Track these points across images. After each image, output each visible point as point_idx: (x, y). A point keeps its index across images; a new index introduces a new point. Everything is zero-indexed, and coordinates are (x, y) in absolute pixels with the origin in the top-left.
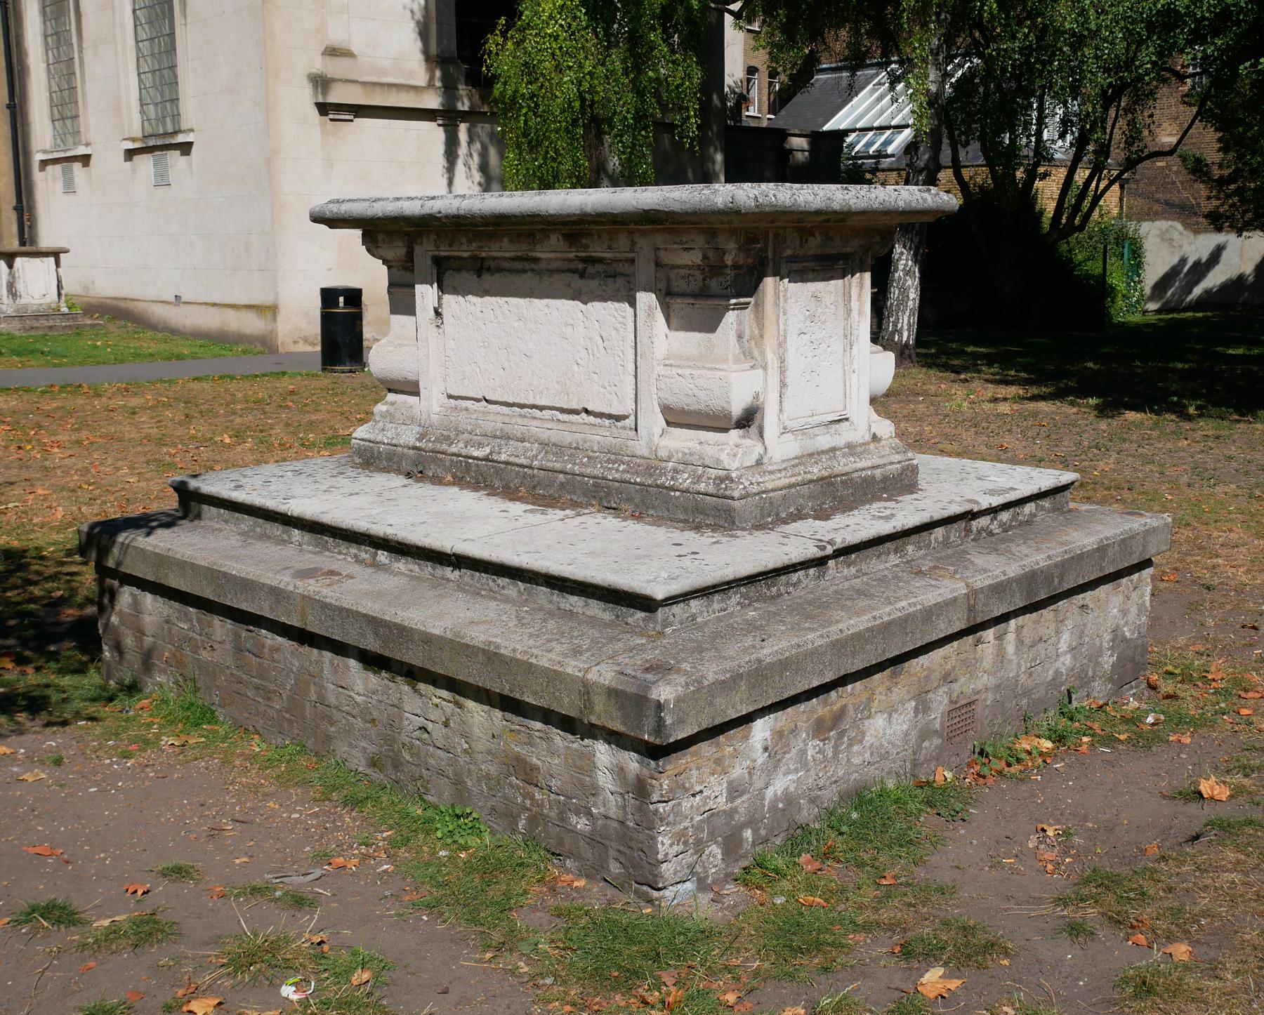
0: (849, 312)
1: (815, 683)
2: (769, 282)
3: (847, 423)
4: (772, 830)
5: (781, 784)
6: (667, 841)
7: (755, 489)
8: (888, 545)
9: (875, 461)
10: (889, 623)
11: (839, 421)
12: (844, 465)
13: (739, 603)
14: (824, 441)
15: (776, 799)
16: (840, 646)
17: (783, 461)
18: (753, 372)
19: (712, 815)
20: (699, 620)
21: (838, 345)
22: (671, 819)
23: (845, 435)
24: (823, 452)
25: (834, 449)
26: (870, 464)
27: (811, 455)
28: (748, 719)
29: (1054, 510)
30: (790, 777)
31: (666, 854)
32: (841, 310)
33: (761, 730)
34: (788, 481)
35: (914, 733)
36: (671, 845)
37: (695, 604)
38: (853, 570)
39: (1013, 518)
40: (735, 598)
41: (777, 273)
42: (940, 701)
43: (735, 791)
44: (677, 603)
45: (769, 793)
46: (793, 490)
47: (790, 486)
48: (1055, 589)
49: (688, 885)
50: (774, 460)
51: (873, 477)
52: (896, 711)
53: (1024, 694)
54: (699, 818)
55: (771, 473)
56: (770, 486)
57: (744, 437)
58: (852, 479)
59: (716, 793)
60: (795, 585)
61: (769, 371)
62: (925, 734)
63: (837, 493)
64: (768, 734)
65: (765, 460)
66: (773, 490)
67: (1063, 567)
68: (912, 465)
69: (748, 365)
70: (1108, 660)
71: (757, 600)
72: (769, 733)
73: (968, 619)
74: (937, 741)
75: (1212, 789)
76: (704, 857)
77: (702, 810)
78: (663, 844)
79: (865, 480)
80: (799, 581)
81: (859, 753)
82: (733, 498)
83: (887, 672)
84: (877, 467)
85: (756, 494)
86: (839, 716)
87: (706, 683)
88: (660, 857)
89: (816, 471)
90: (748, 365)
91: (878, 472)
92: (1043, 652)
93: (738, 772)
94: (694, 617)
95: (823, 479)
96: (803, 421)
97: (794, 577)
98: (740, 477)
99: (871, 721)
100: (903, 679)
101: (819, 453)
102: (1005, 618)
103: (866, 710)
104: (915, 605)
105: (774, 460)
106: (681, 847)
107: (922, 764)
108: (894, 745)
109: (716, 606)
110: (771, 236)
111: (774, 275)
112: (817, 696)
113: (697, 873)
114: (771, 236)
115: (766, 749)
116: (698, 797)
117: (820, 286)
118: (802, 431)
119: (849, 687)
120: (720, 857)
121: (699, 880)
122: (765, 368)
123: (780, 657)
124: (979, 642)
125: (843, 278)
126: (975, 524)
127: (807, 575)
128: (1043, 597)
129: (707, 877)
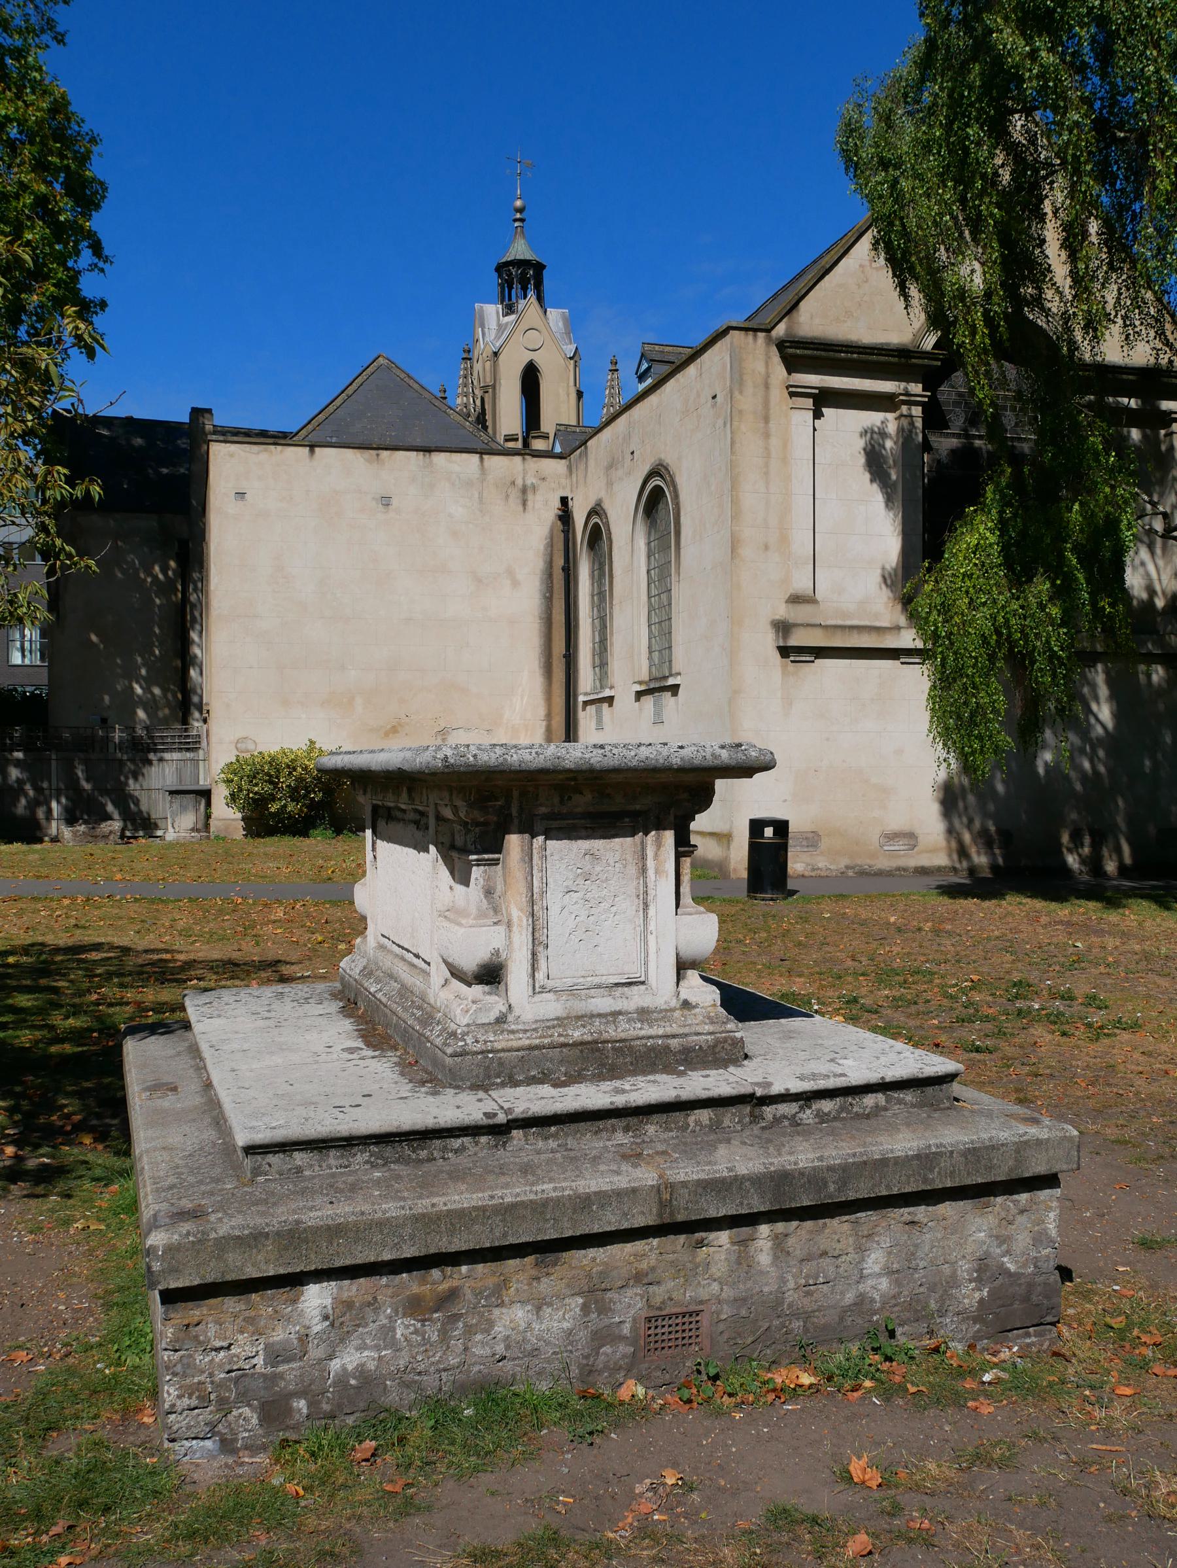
0: (643, 870)
1: (387, 1256)
2: (514, 841)
3: (642, 987)
4: (340, 1406)
5: (349, 1359)
6: (174, 1392)
7: (479, 1047)
8: (613, 1121)
9: (675, 1029)
10: (514, 1206)
11: (630, 984)
12: (624, 1030)
13: (367, 1162)
14: (602, 1003)
15: (344, 1374)
16: (428, 1222)
17: (536, 1021)
18: (497, 927)
19: (242, 1376)
20: (307, 1173)
21: (628, 906)
22: (179, 1369)
23: (636, 999)
24: (600, 1015)
25: (616, 1014)
26: (661, 1032)
27: (579, 1018)
28: (296, 1280)
29: (920, 1105)
30: (366, 1353)
31: (173, 1405)
32: (632, 870)
33: (316, 1298)
34: (527, 1042)
35: (583, 1335)
36: (179, 1397)
37: (299, 1158)
38: (552, 1144)
39: (842, 1109)
40: (360, 1157)
41: (529, 829)
42: (629, 1307)
43: (276, 1356)
44: (276, 1152)
45: (335, 1365)
46: (536, 1052)
47: (531, 1048)
48: (830, 1197)
49: (208, 1444)
50: (523, 1018)
51: (668, 1047)
52: (550, 1305)
53: (796, 1315)
54: (223, 1375)
55: (513, 1032)
56: (498, 1046)
57: (490, 993)
58: (631, 1047)
59: (248, 1351)
60: (456, 1151)
61: (515, 929)
62: (602, 1337)
63: (598, 1057)
64: (328, 1302)
65: (510, 1018)
66: (503, 1050)
67: (846, 1172)
68: (733, 1039)
69: (490, 921)
70: (970, 1296)
71: (397, 1161)
72: (330, 1301)
73: (660, 1215)
74: (625, 1349)
75: (864, 1471)
76: (230, 1417)
77: (228, 1368)
78: (169, 1394)
79: (653, 1049)
80: (463, 1148)
81: (483, 1344)
82: (444, 1053)
83: (530, 1260)
84: (674, 1036)
85: (477, 1053)
86: (452, 1295)
87: (213, 1235)
88: (166, 1406)
89: (577, 1034)
90: (490, 921)
91: (674, 1043)
92: (832, 1269)
93: (279, 1335)
94: (299, 1170)
95: (582, 1043)
96: (570, 982)
97: (456, 1143)
98: (465, 1034)
99: (504, 1310)
100: (558, 1271)
101: (592, 1016)
102: (751, 1220)
103: (497, 1296)
104: (563, 1189)
105: (523, 1018)
106: (194, 1402)
107: (600, 1372)
108: (548, 1343)
109: (332, 1162)
110: (516, 794)
111: (521, 832)
112: (409, 1271)
113: (219, 1433)
114: (516, 794)
115: (326, 1318)
116: (222, 1353)
117: (598, 844)
118: (572, 991)
119: (464, 1269)
120: (255, 1421)
121: (223, 1441)
122: (509, 925)
123: (330, 1222)
124: (701, 1244)
125: (633, 836)
126: (769, 1111)
127: (477, 1143)
128: (806, 1203)
129: (236, 1440)
